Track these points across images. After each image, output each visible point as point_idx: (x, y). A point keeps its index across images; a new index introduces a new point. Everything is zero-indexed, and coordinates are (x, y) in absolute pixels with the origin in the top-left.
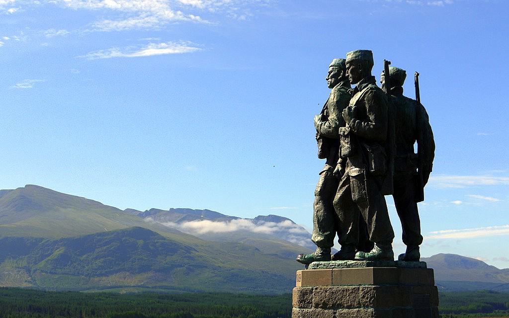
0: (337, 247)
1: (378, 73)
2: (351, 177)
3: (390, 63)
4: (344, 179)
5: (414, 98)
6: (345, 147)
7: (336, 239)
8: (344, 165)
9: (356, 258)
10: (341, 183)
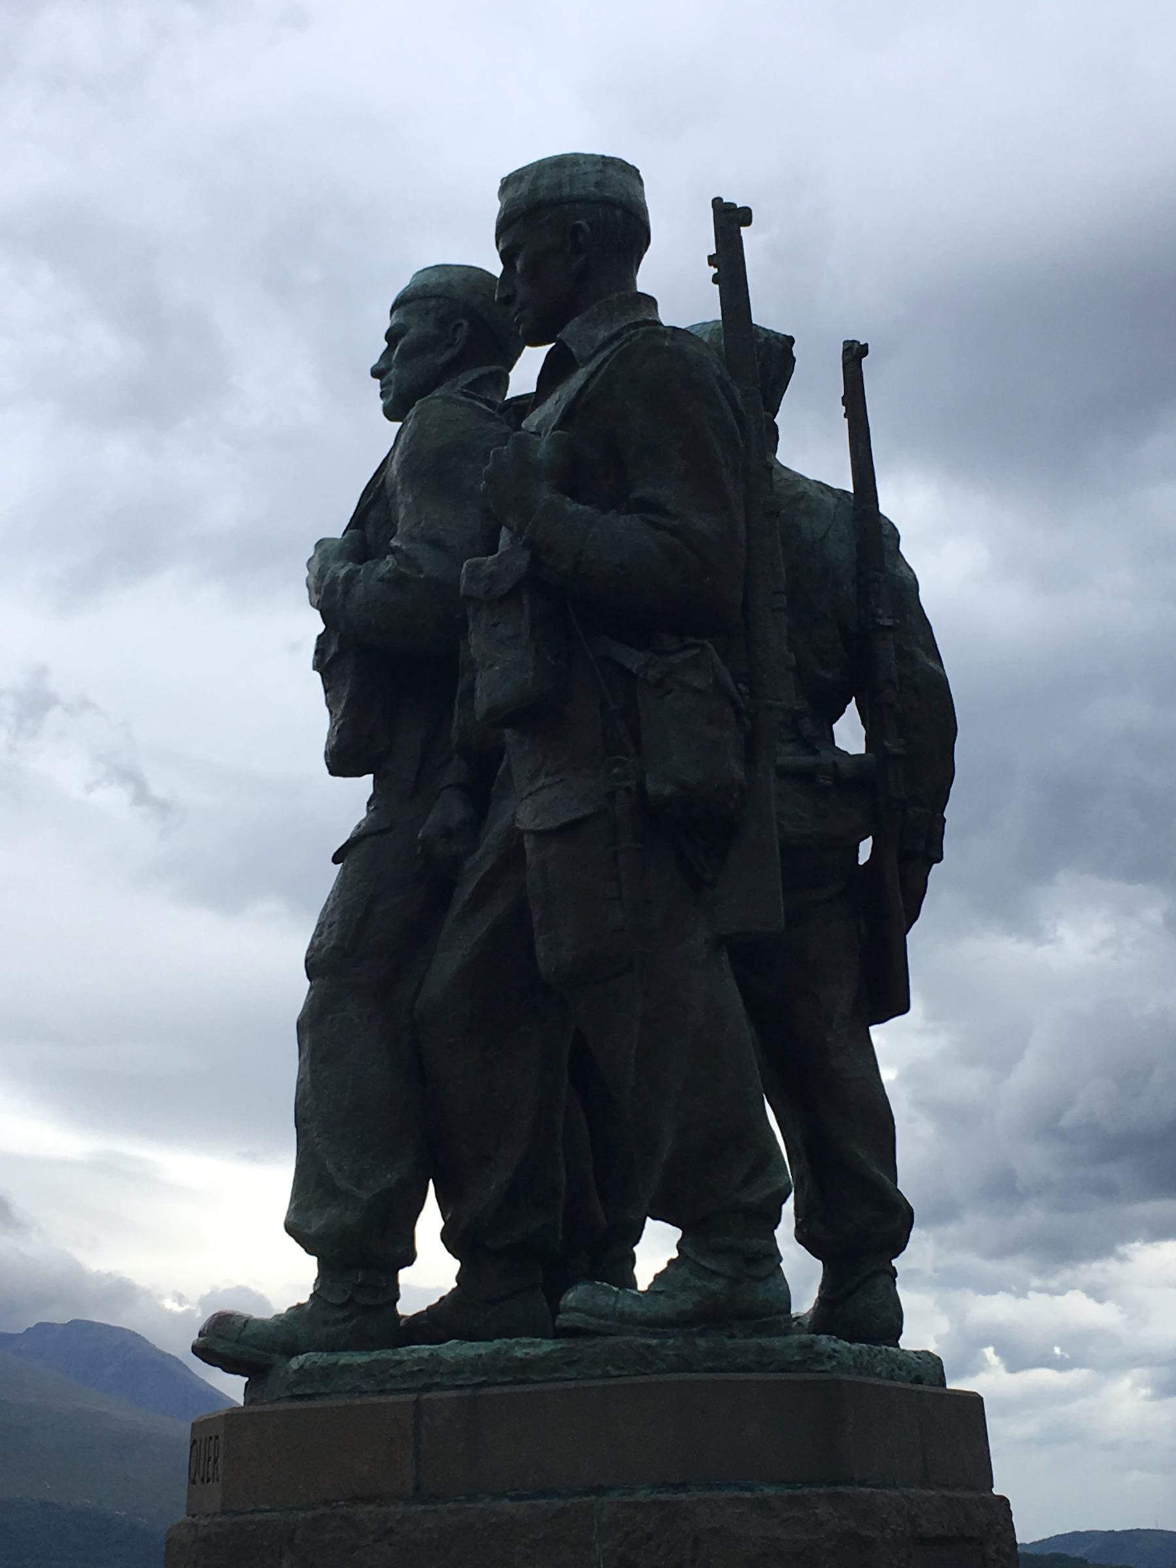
0: (430, 1273)
1: (675, 280)
2: (529, 845)
3: (744, 216)
4: (481, 862)
5: (847, 484)
6: (497, 666)
7: (430, 1222)
8: (482, 786)
9: (563, 1319)
10: (465, 891)
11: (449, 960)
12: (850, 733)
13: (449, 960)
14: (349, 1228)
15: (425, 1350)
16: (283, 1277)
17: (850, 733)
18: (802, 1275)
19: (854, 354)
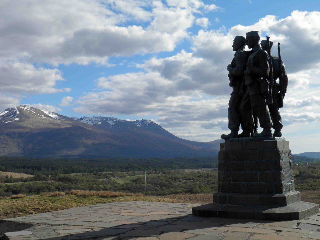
0: (240, 132)
3: (269, 38)
5: (278, 56)
7: (240, 127)
10: (243, 99)
11: (242, 104)
12: (278, 81)
13: (242, 104)
14: (233, 126)
15: (242, 138)
16: (228, 132)
17: (278, 81)
18: (273, 131)
19: (279, 44)
